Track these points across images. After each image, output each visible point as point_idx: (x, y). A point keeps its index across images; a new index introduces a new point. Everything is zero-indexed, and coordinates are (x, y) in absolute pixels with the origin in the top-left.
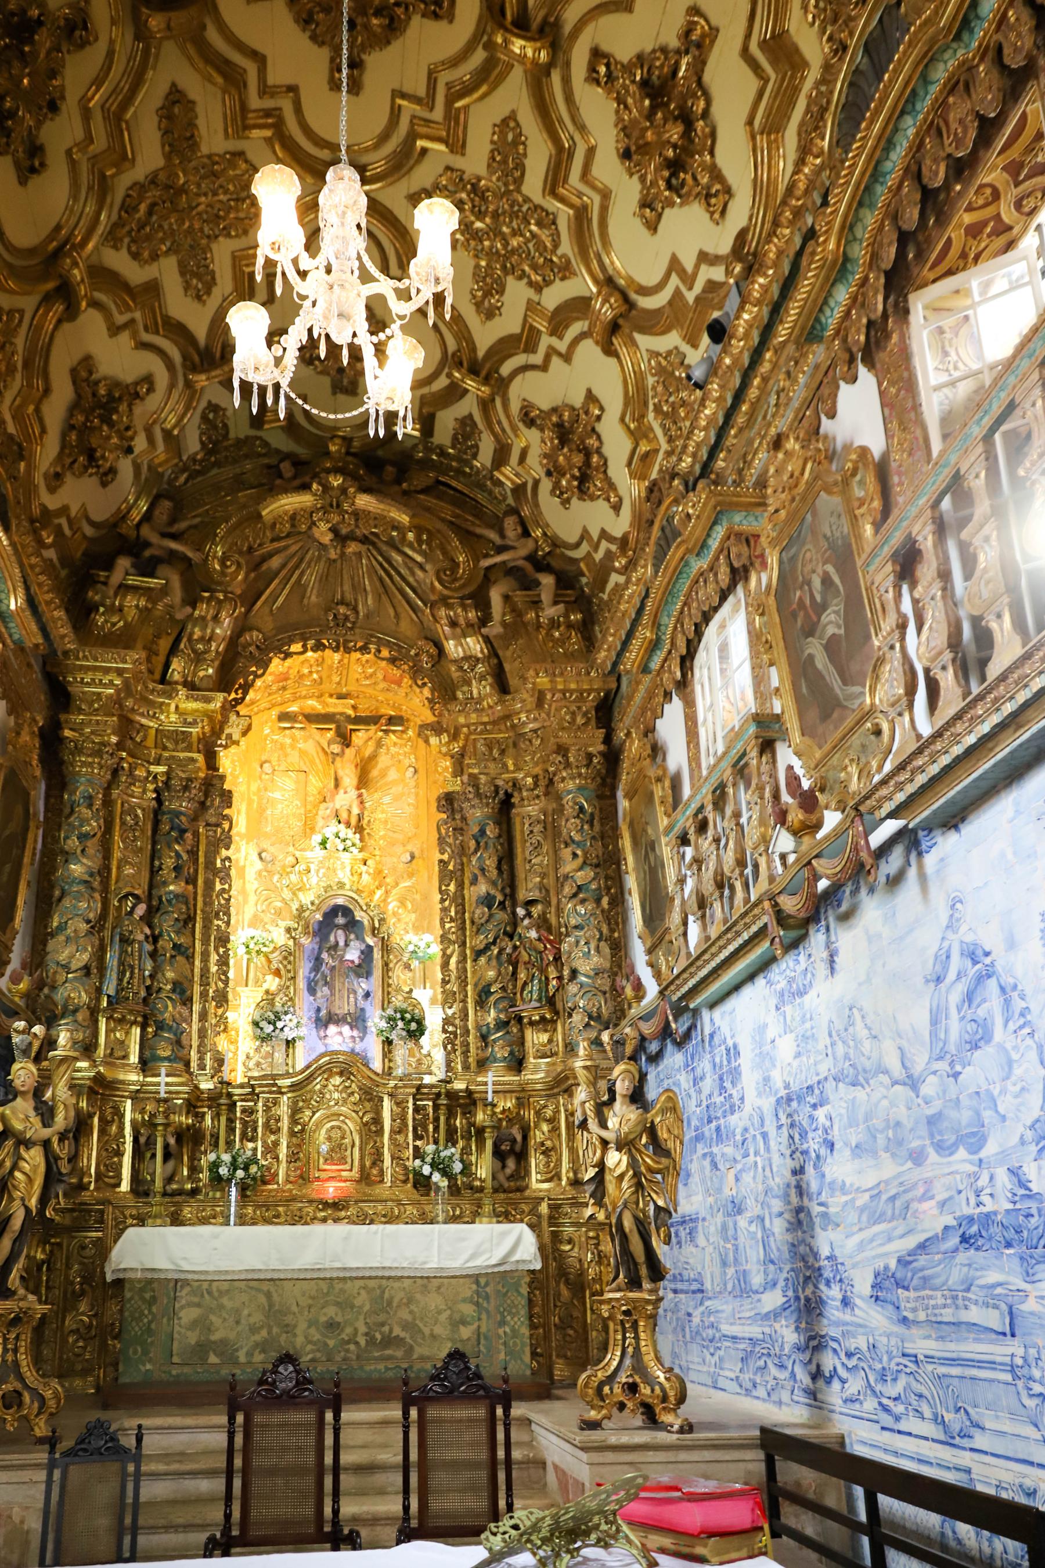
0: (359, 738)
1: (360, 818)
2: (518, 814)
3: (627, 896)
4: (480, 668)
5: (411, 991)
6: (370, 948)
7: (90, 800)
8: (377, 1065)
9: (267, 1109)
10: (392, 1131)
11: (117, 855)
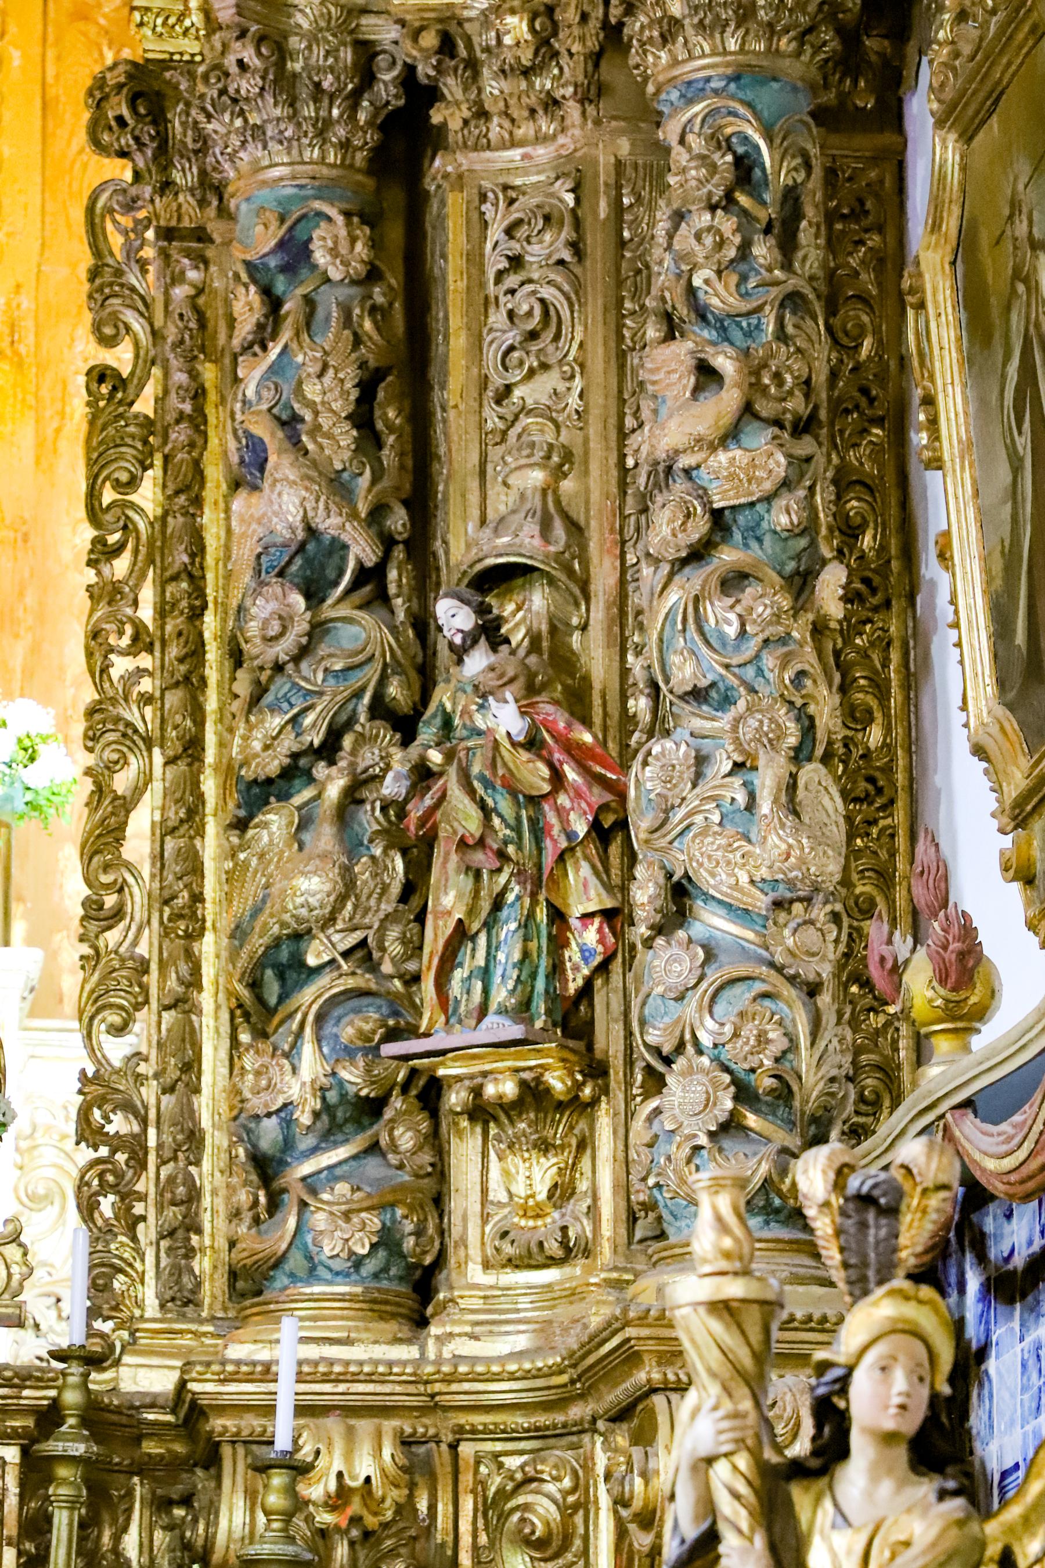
2: (459, 181)
3: (930, 568)
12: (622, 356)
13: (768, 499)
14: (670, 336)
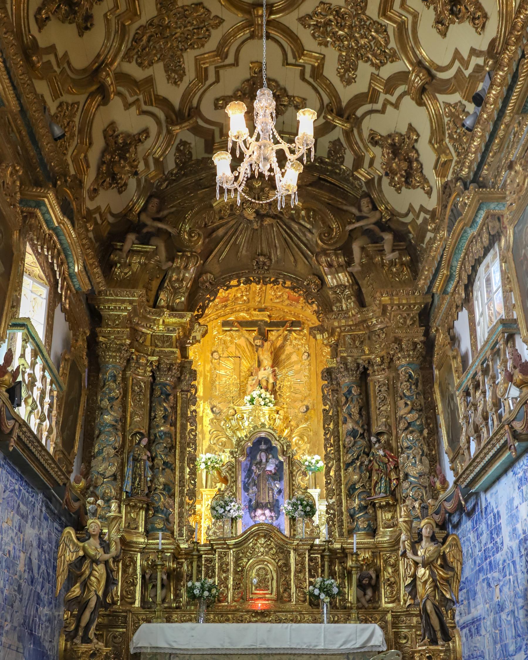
0: (273, 335)
1: (274, 385)
2: (372, 380)
4: (347, 292)
5: (307, 488)
6: (281, 463)
7: (115, 377)
8: (287, 533)
9: (221, 558)
10: (296, 571)
11: (130, 409)
12: (395, 403)
13: (416, 420)
14: (401, 399)
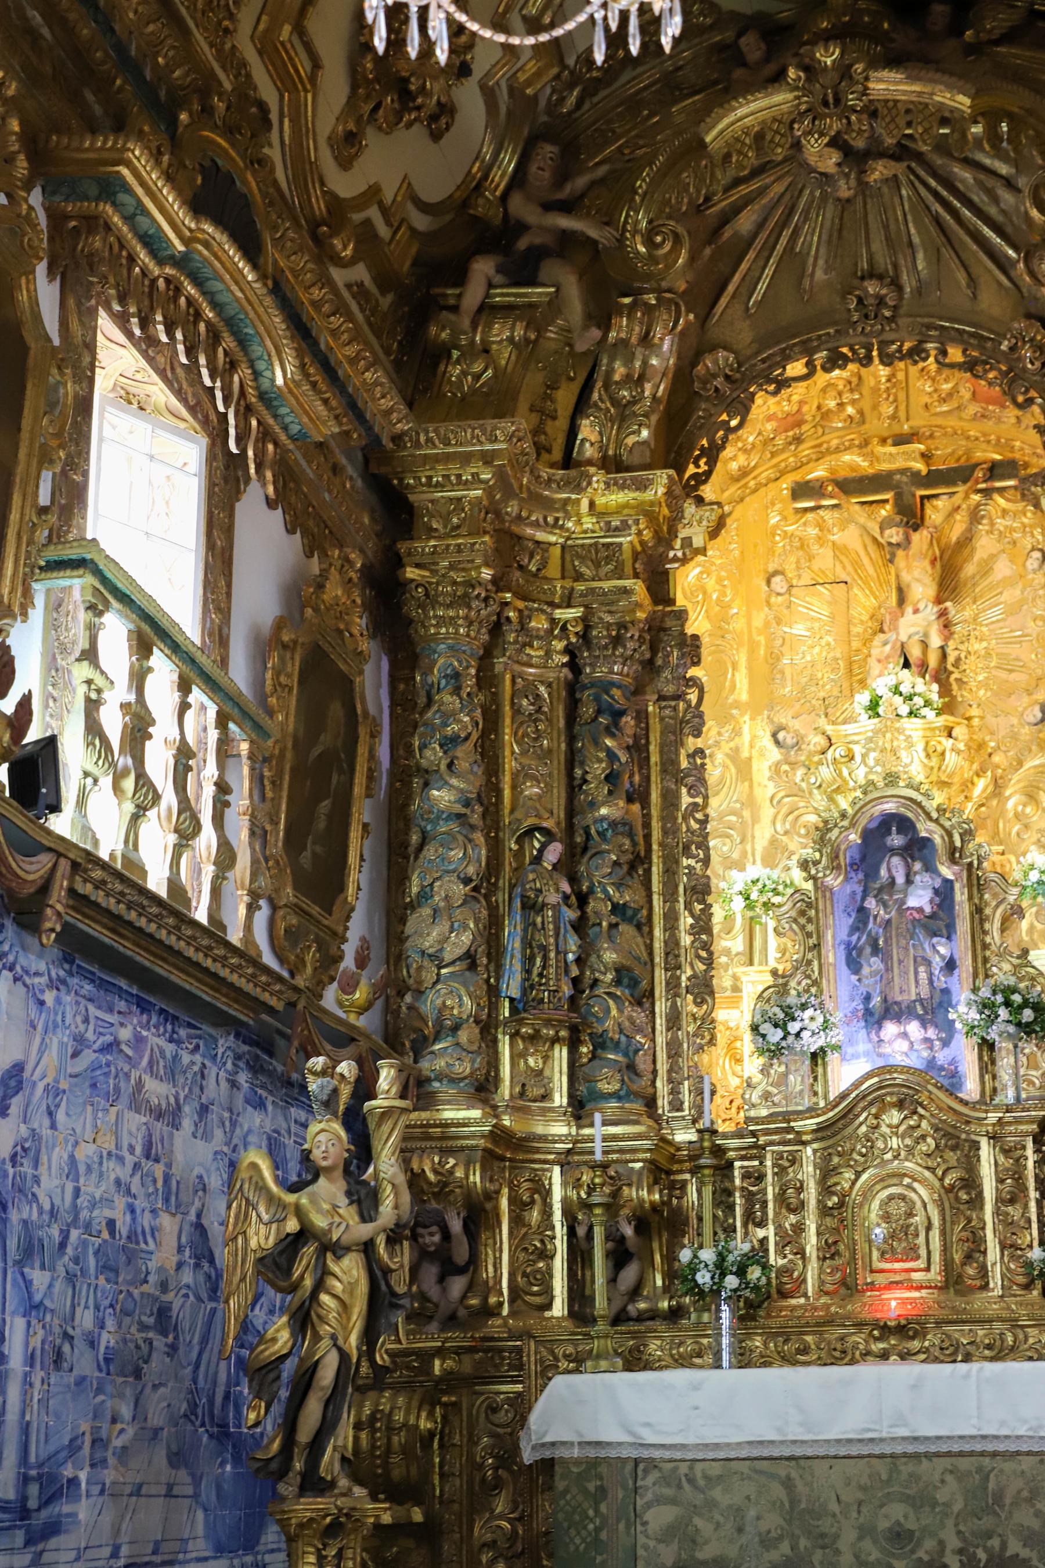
7: (456, 675)
9: (781, 1171)
11: (509, 765)
